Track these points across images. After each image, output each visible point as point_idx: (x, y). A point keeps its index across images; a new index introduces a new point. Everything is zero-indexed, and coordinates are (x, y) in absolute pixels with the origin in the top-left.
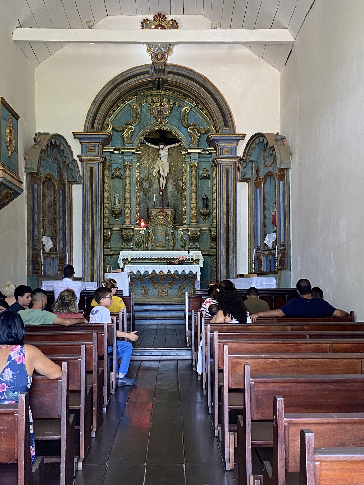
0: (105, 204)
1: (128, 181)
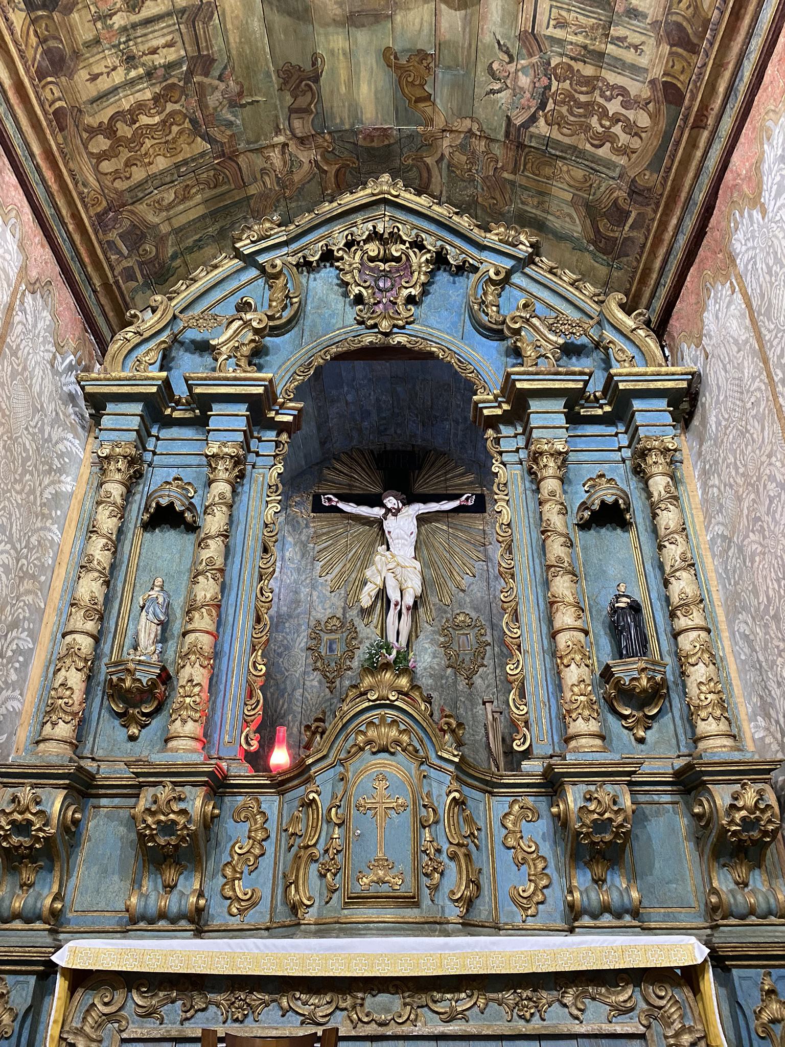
0: (69, 638)
1: (214, 523)
